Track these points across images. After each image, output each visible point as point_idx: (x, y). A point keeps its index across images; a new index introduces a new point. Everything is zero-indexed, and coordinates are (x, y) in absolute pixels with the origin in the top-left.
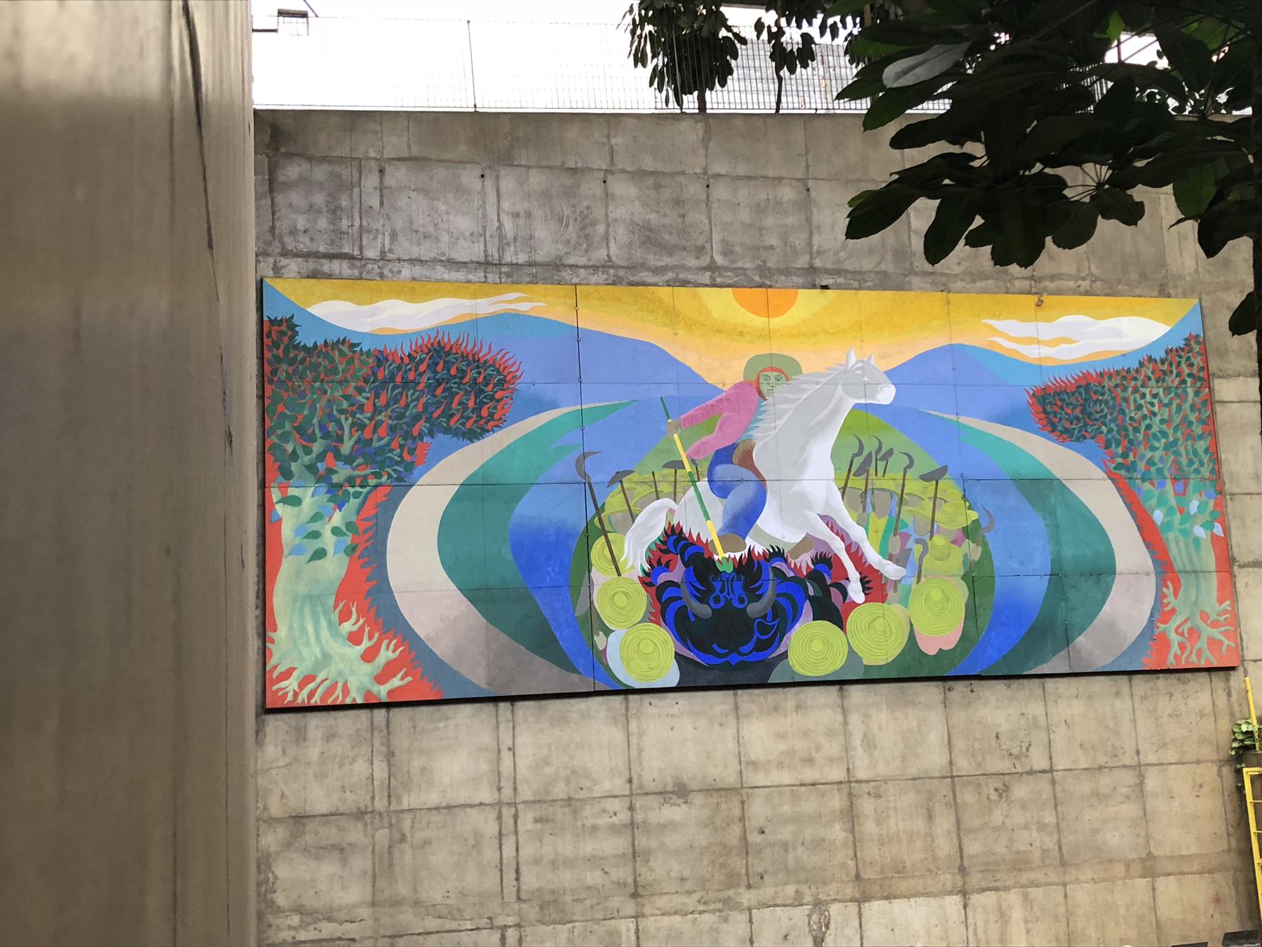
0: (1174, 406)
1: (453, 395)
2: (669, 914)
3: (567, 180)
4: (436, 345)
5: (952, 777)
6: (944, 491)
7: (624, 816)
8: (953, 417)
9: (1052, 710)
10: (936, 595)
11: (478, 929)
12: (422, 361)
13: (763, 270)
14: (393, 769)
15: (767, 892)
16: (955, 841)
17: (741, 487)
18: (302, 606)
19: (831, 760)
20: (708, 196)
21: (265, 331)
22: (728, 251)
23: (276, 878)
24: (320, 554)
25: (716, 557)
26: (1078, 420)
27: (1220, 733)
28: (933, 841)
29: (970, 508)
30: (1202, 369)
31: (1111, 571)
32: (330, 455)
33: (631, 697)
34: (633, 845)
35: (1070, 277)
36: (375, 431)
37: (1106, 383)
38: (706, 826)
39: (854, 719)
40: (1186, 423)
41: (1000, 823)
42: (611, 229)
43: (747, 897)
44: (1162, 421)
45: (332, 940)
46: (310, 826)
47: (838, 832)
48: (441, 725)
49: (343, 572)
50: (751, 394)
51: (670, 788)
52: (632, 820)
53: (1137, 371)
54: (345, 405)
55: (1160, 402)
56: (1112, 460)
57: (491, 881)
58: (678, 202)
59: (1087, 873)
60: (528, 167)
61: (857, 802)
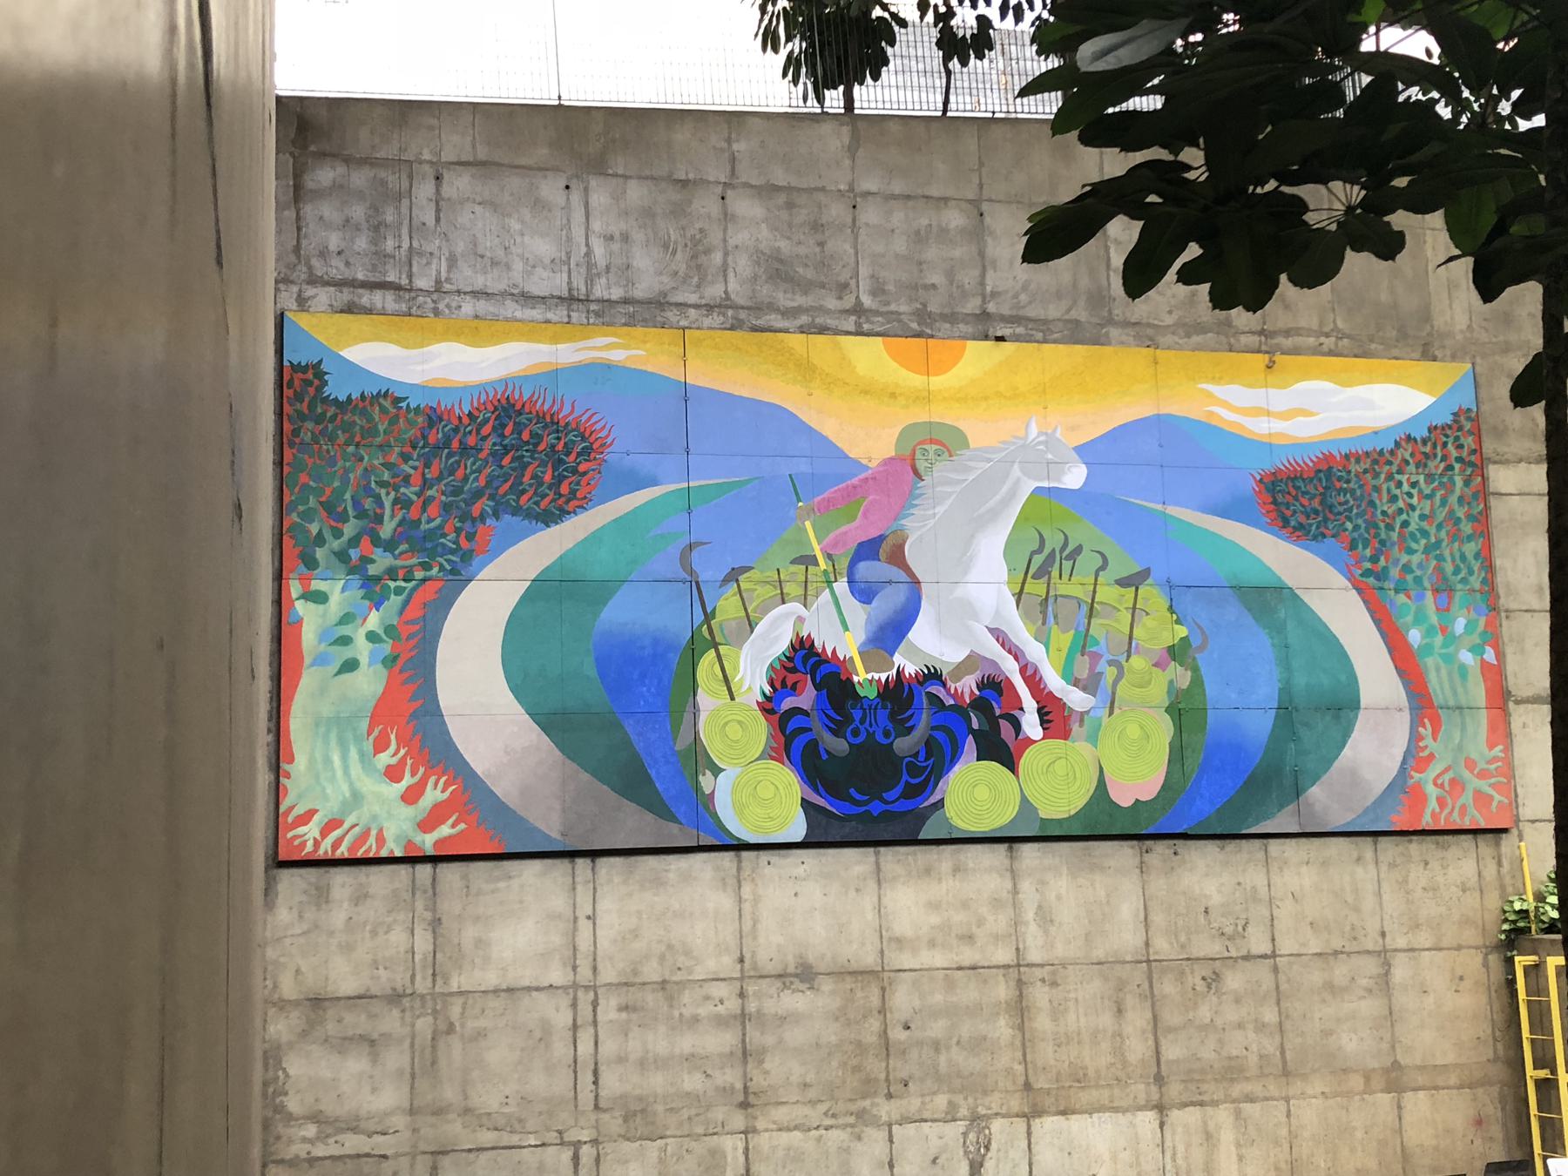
1: (525, 466)
2: (789, 1129)
3: (674, 195)
4: (504, 402)
5: (1148, 961)
6: (1146, 600)
7: (733, 1005)
8: (1159, 507)
9: (1276, 879)
10: (1133, 731)
11: (543, 1145)
12: (486, 421)
13: (923, 315)
14: (440, 939)
15: (912, 1104)
16: (1151, 1042)
17: (889, 589)
18: (328, 731)
19: (996, 938)
20: (854, 220)
21: (286, 378)
22: (878, 290)
23: (287, 1076)
24: (350, 666)
25: (856, 679)
26: (1317, 513)
27: (1487, 910)
28: (1122, 1042)
29: (1178, 622)
30: (1474, 452)
31: (1354, 705)
32: (365, 540)
33: (745, 854)
34: (744, 1041)
35: (1309, 332)
36: (424, 509)
37: (1354, 468)
38: (837, 1019)
39: (1026, 886)
40: (1452, 518)
41: (1208, 1021)
42: (730, 259)
43: (886, 1110)
44: (1422, 517)
45: (358, 1156)
46: (331, 1013)
47: (1003, 1029)
48: (502, 885)
49: (381, 690)
50: (905, 471)
51: (791, 969)
52: (743, 1009)
53: (1392, 452)
54: (386, 476)
55: (1420, 492)
56: (1358, 564)
57: (562, 1084)
58: (817, 227)
59: (1317, 1085)
60: (626, 177)
61: (1027, 991)
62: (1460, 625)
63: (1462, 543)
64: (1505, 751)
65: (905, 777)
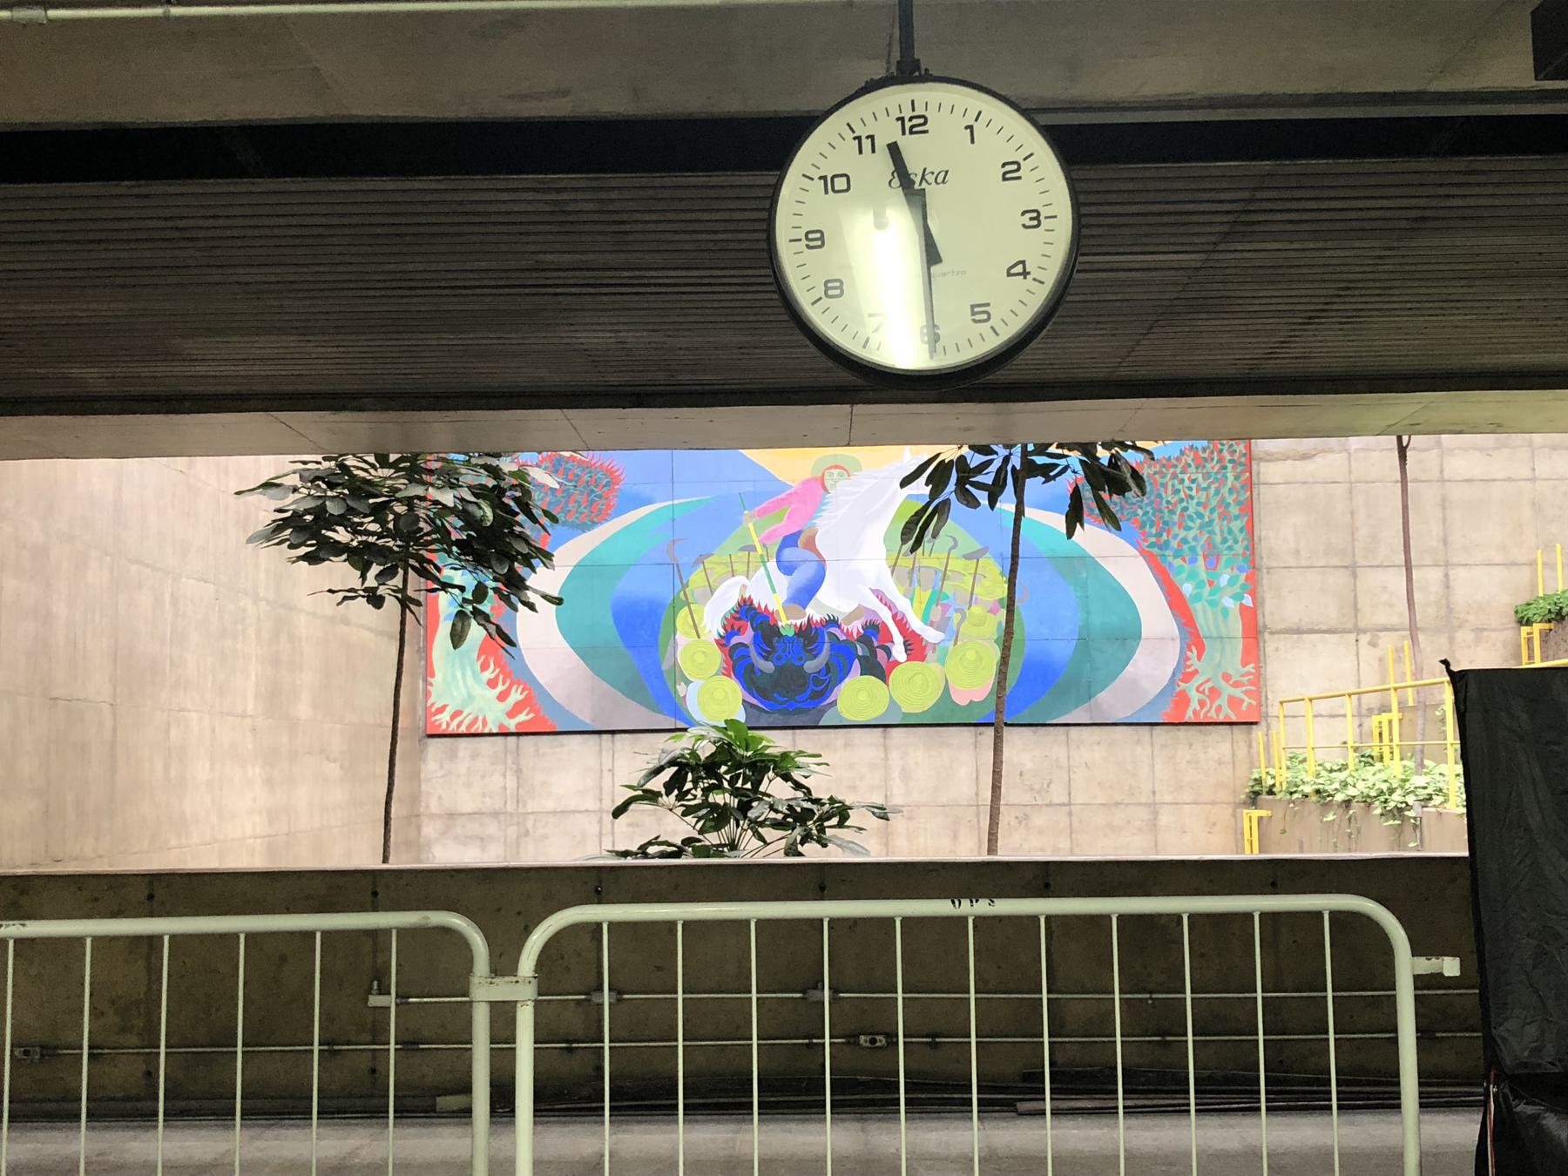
0: (1212, 490)
10: (971, 656)
39: (895, 755)
40: (1223, 504)
44: (1198, 504)
53: (1178, 459)
62: (1224, 580)
63: (1229, 521)
64: (1258, 668)
65: (811, 686)
